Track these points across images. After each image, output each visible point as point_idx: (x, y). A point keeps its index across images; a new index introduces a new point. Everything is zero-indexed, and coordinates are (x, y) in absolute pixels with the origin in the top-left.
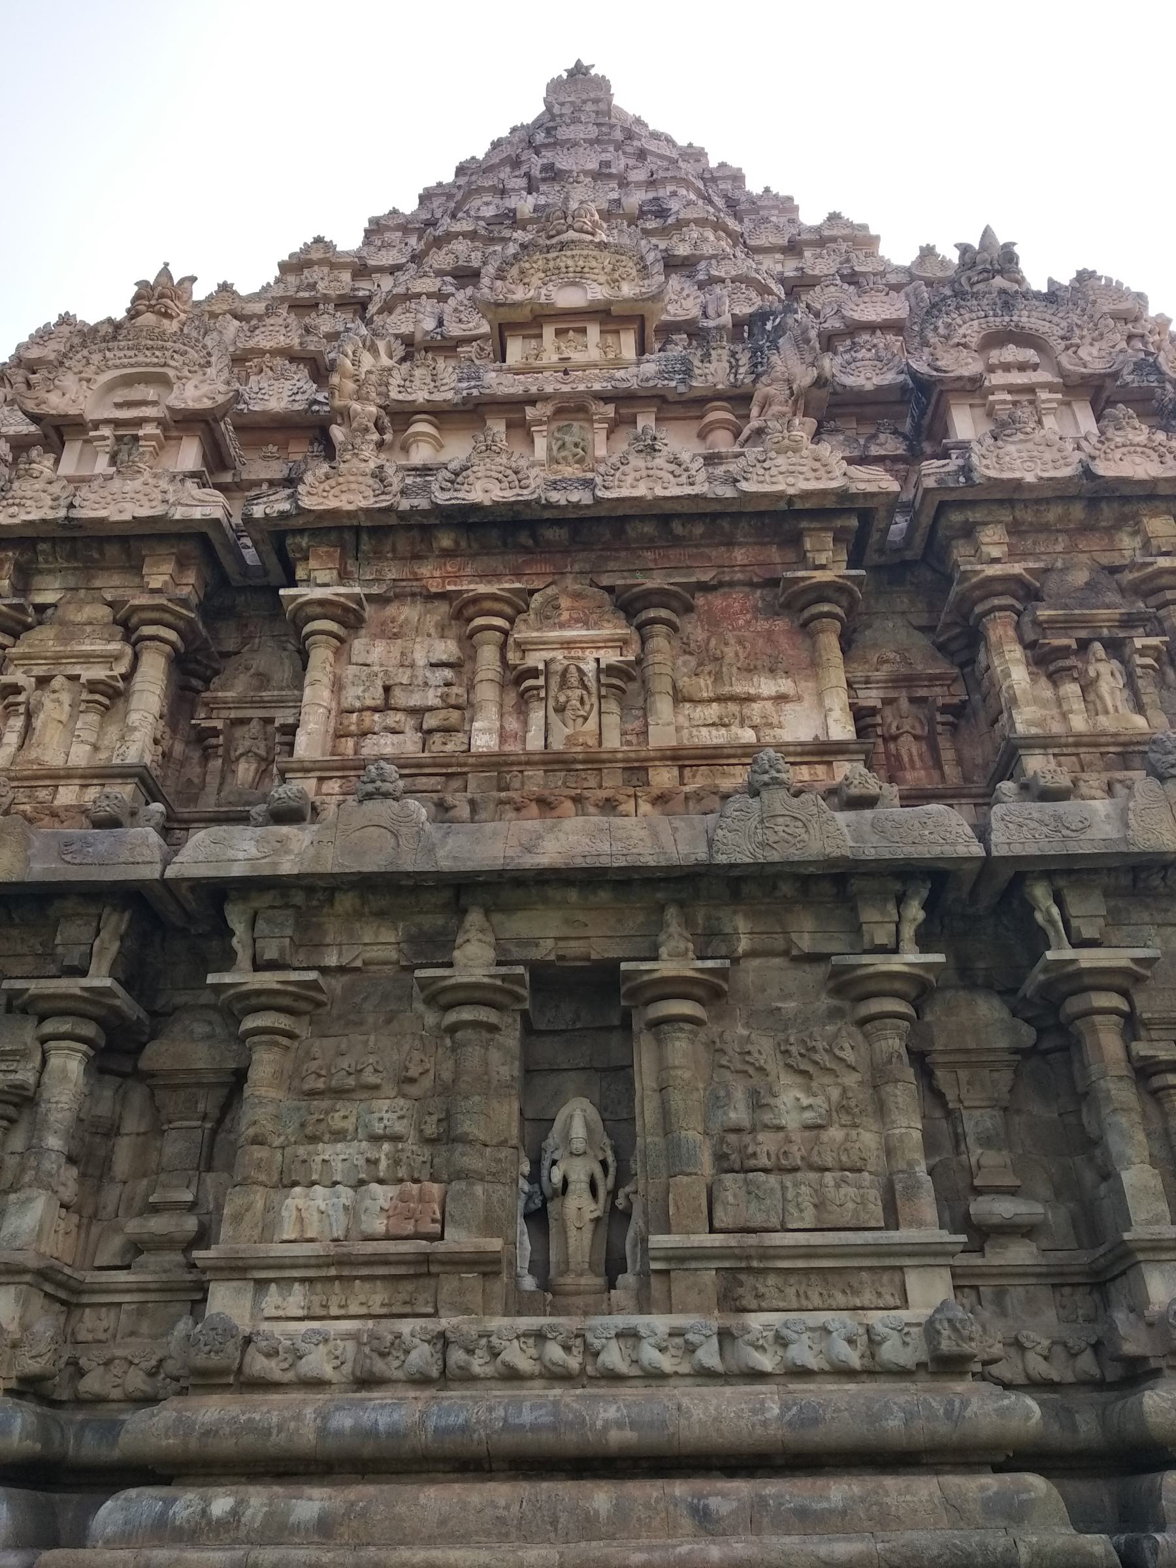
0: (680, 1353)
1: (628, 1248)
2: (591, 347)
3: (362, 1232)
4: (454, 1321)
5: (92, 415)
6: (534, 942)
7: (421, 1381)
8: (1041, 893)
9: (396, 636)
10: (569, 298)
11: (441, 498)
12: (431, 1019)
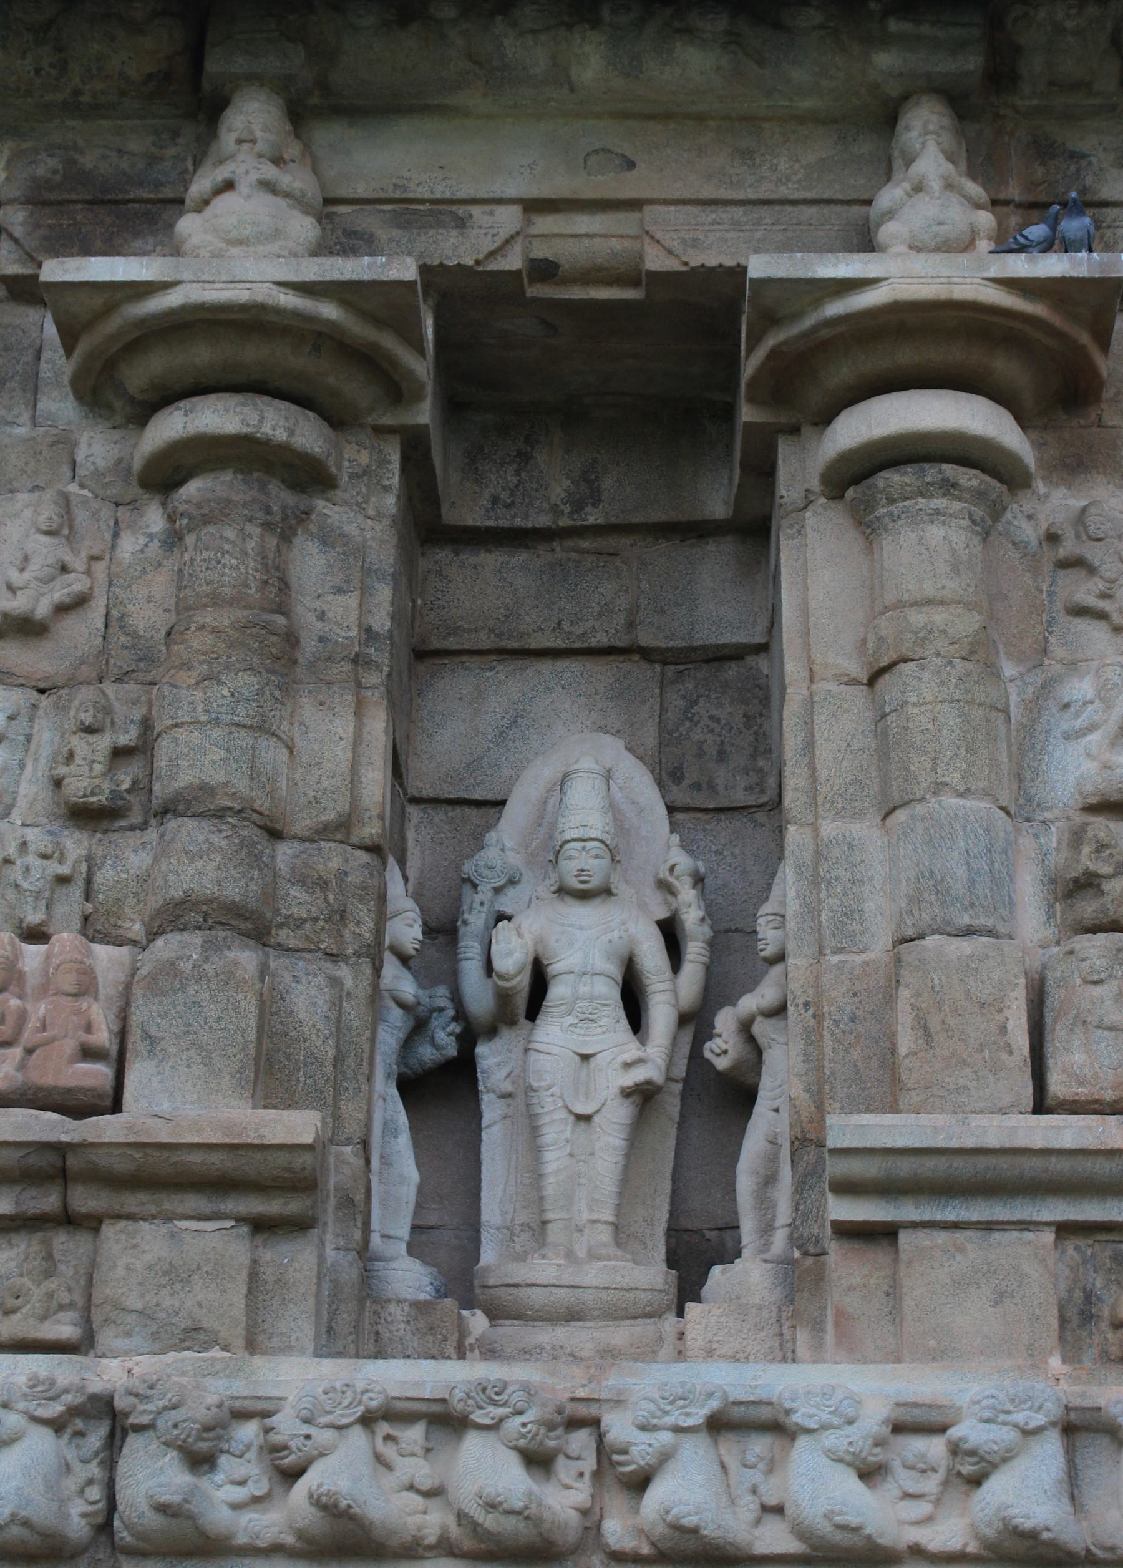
0: (931, 1484)
1: (745, 1183)
4: (146, 1365)
6: (448, 212)
12: (97, 447)
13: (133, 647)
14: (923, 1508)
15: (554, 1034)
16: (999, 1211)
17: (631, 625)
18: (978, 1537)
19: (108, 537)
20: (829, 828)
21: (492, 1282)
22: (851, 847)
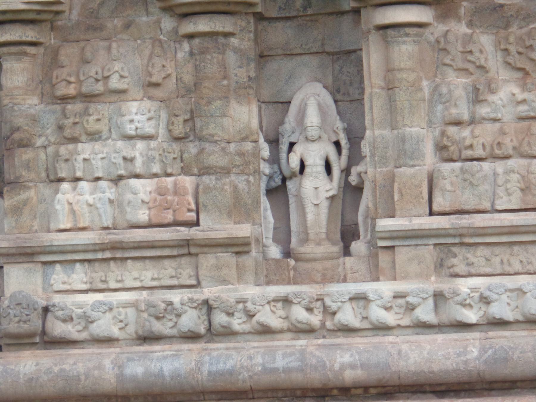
0: (402, 310)
3: (128, 221)
7: (192, 337)
13: (185, 87)
14: (401, 316)
16: (419, 242)
17: (323, 45)
18: (413, 322)
19: (173, 52)
20: (377, 132)
21: (295, 252)
22: (383, 138)
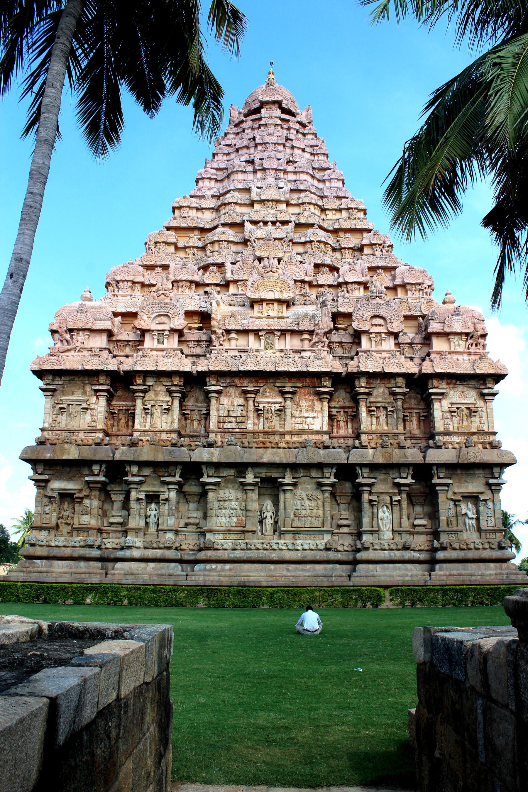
2: (275, 310)
5: (152, 329)
7: (243, 550)
8: (357, 468)
9: (230, 396)
10: (270, 296)
11: (241, 368)
12: (241, 487)
15: (267, 520)
